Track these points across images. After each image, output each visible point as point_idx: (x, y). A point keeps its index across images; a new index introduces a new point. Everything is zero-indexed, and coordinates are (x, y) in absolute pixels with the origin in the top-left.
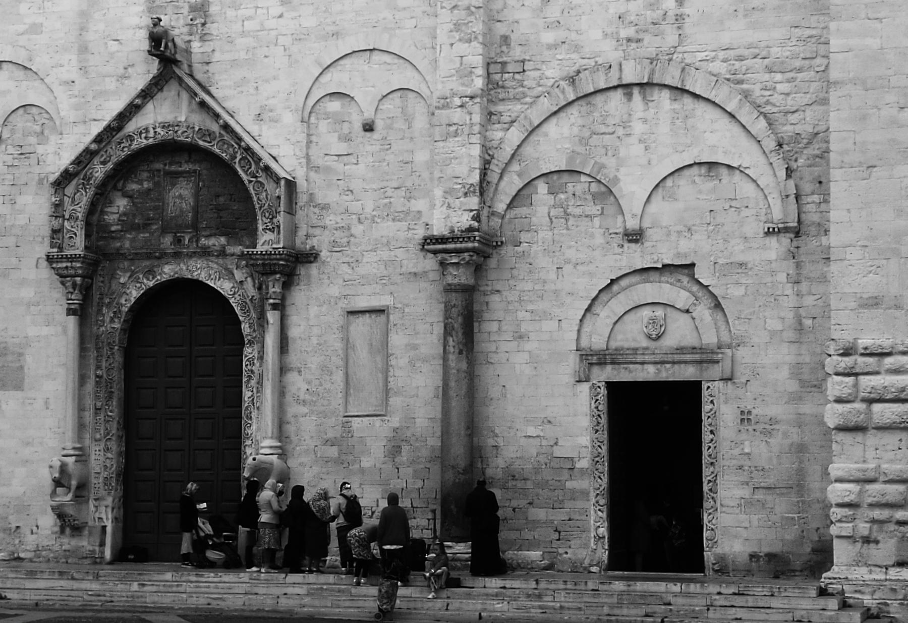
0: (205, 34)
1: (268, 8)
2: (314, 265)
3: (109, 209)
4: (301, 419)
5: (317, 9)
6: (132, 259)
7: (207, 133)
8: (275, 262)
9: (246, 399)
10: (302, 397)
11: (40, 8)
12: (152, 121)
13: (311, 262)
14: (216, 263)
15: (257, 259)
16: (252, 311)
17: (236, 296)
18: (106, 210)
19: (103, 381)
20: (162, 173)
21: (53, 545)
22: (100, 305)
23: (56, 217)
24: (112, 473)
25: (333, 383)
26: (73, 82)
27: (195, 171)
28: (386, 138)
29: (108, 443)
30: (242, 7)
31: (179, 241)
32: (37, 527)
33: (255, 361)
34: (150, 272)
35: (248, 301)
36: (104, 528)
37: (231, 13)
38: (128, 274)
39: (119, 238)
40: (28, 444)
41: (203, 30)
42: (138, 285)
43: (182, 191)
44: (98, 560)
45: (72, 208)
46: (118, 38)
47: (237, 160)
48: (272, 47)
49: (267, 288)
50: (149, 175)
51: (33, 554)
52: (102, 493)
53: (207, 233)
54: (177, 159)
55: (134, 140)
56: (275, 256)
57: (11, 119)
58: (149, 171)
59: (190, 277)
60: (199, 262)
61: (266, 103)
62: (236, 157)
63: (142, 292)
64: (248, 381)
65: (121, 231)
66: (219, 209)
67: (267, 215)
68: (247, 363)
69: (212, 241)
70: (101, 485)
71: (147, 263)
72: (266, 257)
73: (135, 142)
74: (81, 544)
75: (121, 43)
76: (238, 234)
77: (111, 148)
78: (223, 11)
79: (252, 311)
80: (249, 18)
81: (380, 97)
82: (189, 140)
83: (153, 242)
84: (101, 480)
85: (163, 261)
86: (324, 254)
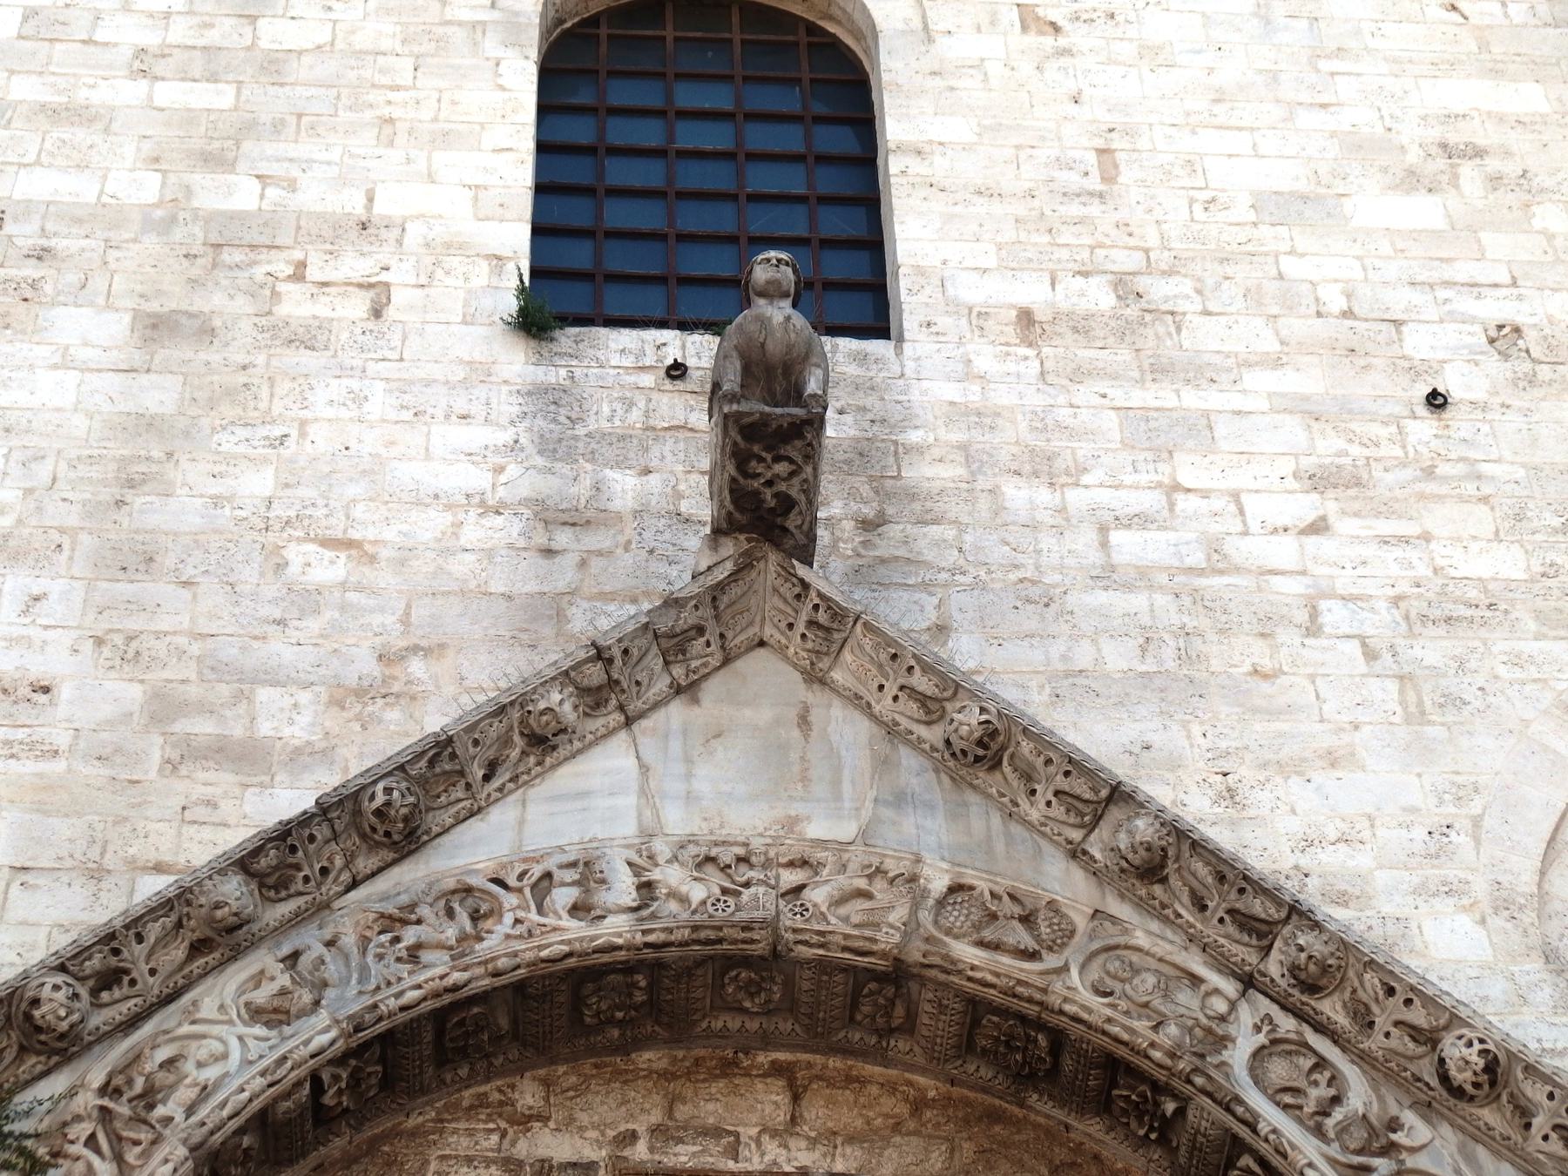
5: (1519, 518)
7: (1008, 907)
12: (627, 829)
26: (46, 690)
30: (1086, 479)
41: (864, 543)
46: (355, 535)
47: (1239, 1055)
48: (1288, 637)
54: (709, 1107)
55: (496, 912)
61: (1304, 861)
75: (372, 559)
77: (330, 944)
78: (982, 483)
80: (1140, 521)
82: (887, 939)
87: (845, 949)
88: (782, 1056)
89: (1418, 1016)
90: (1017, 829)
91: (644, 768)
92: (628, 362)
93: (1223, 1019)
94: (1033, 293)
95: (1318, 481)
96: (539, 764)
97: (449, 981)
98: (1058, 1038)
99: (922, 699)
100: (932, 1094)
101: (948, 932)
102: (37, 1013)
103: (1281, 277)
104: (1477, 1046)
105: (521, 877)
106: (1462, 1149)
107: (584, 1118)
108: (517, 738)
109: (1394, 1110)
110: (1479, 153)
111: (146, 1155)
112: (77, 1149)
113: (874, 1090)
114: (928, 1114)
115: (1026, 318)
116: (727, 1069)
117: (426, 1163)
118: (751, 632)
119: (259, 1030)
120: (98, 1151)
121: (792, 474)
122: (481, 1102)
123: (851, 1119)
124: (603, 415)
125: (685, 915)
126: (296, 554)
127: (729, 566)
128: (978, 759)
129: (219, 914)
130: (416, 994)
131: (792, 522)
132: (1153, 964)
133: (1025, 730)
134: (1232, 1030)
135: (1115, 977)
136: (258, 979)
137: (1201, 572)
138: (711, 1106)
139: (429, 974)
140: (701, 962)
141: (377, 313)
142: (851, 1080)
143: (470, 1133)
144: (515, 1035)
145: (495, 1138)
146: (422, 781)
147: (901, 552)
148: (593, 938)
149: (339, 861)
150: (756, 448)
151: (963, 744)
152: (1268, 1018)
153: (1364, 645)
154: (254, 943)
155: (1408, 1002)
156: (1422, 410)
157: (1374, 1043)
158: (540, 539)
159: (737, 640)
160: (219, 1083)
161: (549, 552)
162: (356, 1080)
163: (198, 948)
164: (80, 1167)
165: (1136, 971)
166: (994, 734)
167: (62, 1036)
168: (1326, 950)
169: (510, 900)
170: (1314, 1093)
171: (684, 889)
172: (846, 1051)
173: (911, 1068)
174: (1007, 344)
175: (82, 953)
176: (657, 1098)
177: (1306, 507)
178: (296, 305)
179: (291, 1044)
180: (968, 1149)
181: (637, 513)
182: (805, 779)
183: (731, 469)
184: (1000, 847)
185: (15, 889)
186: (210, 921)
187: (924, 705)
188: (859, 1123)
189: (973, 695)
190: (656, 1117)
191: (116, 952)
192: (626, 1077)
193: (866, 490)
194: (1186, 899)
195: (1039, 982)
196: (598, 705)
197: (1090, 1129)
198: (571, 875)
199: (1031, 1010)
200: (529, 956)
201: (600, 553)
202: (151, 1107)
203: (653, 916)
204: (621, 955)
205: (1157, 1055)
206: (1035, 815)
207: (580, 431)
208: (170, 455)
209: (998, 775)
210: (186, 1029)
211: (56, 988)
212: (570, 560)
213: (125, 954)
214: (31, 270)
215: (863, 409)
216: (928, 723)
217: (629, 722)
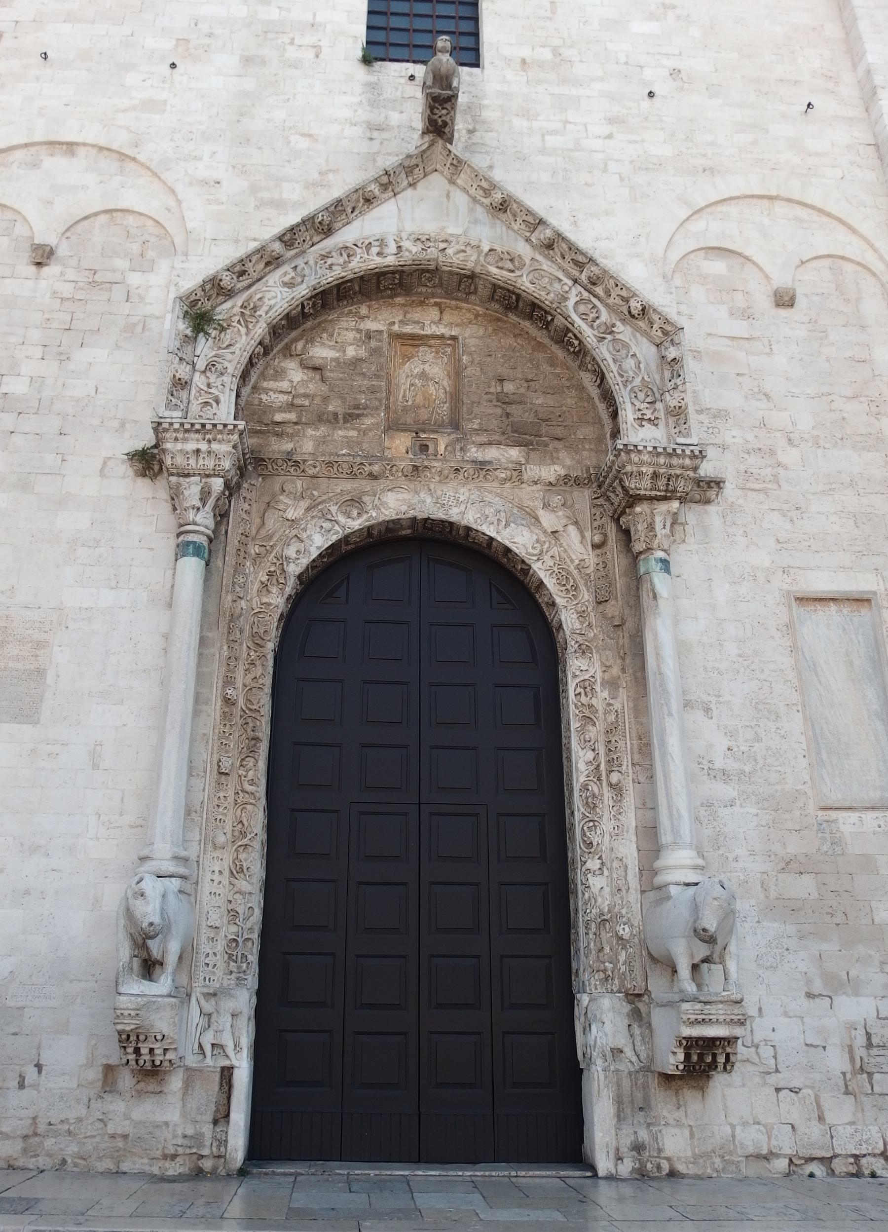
0: (474, 144)
1: (585, 125)
2: (711, 508)
3: (272, 384)
4: (723, 812)
6: (314, 477)
7: (506, 256)
8: (678, 472)
9: (582, 766)
10: (719, 764)
11: (163, 82)
12: (394, 229)
13: (708, 502)
14: (500, 496)
15: (642, 463)
16: (582, 587)
17: (546, 558)
18: (265, 384)
19: (237, 712)
20: (385, 335)
21: (79, 1120)
22: (242, 552)
23: (181, 359)
24: (251, 930)
25: (783, 737)
26: (219, 183)
27: (454, 338)
28: (816, 322)
29: (242, 856)
30: (540, 118)
31: (424, 448)
32: (39, 1067)
33: (598, 687)
34: (355, 502)
35: (572, 568)
36: (227, 1073)
37: (519, 123)
38: (304, 504)
39: (291, 436)
40: (35, 849)
41: (469, 138)
42: (327, 525)
43: (427, 367)
44: (207, 1165)
45: (214, 353)
46: (311, 132)
47: (571, 303)
49: (651, 527)
50: (358, 336)
51: (19, 1145)
52: (219, 978)
53: (483, 438)
55: (355, 254)
56: (681, 461)
57: (80, 227)
58: (359, 331)
59: (443, 517)
60: (462, 490)
62: (566, 299)
63: (334, 538)
64: (582, 730)
65: (296, 423)
66: (503, 400)
67: (641, 396)
68: (579, 690)
69: (491, 453)
70: (220, 960)
71: (349, 485)
72: (662, 460)
73: (357, 259)
74: (159, 1118)
75: (316, 141)
76: (546, 445)
77: (306, 263)
79: (582, 587)
80: (554, 132)
81: (798, 262)
82: (470, 265)
83: (365, 446)
84: (220, 946)
85: (382, 484)
86: (729, 489)
87: (458, 268)
88: (438, 300)
89: (624, 293)
90: (510, 232)
91: (399, 210)
92: (397, 74)
93: (567, 292)
94: (526, 52)
95: (611, 121)
96: (368, 208)
97: (341, 276)
98: (518, 297)
99: (484, 190)
100: (481, 313)
101: (488, 263)
102: (221, 284)
103: (606, 49)
104: (640, 303)
105: (362, 244)
106: (632, 333)
107: (380, 317)
108: (361, 199)
109: (614, 321)
110: (674, 7)
111: (254, 326)
112: (235, 324)
113: (464, 311)
114: (479, 318)
115: (524, 62)
116: (422, 303)
117: (334, 330)
118: (433, 167)
119: (286, 289)
120: (241, 325)
121: (448, 114)
122: (350, 312)
123: (456, 319)
124: (388, 93)
125: (411, 257)
126: (294, 138)
127: (427, 145)
128: (500, 209)
129: (273, 254)
130: (331, 279)
131: (447, 130)
132: (548, 275)
133: (515, 201)
134: (569, 296)
135: (536, 279)
136: (285, 274)
137: (572, 150)
138: (417, 315)
139: (335, 273)
140: (415, 271)
141: (317, 56)
142: (458, 308)
143: (347, 321)
144: (360, 292)
145: (354, 323)
146: (333, 213)
147: (480, 141)
148: (383, 263)
149: (308, 238)
150: (437, 105)
151: (496, 205)
152: (580, 292)
153: (620, 176)
154: (284, 263)
155: (622, 289)
156: (646, 97)
157: (610, 301)
158: (368, 135)
159: (428, 169)
160: (275, 305)
161: (371, 139)
162: (314, 305)
163: (268, 264)
164: (236, 329)
165: (543, 277)
166: (505, 201)
167: (229, 290)
168: (599, 272)
169: (358, 251)
170: (592, 315)
171: (410, 248)
172: (457, 299)
173: (475, 305)
174: (517, 71)
175: (234, 266)
176: (401, 312)
177: (606, 129)
178: (292, 53)
179: (296, 293)
180: (490, 329)
181: (399, 126)
182: (448, 215)
183: (429, 112)
184: (505, 238)
185: (213, 246)
186: (271, 256)
187: (484, 191)
188: (459, 321)
189: (500, 189)
190: (401, 317)
191: (243, 265)
192: (393, 305)
193: (470, 120)
194: (559, 255)
195: (514, 279)
196: (385, 190)
197: (526, 324)
198: (377, 243)
199: (511, 288)
200: (364, 268)
201: (387, 140)
202: (255, 312)
203: (401, 257)
204: (392, 268)
205: (547, 302)
206: (516, 228)
207: (381, 98)
208: (253, 105)
209: (506, 215)
210: (265, 289)
211: (227, 276)
212: (376, 143)
213: (246, 266)
214: (207, 41)
215: (470, 92)
216: (486, 197)
217: (395, 195)
